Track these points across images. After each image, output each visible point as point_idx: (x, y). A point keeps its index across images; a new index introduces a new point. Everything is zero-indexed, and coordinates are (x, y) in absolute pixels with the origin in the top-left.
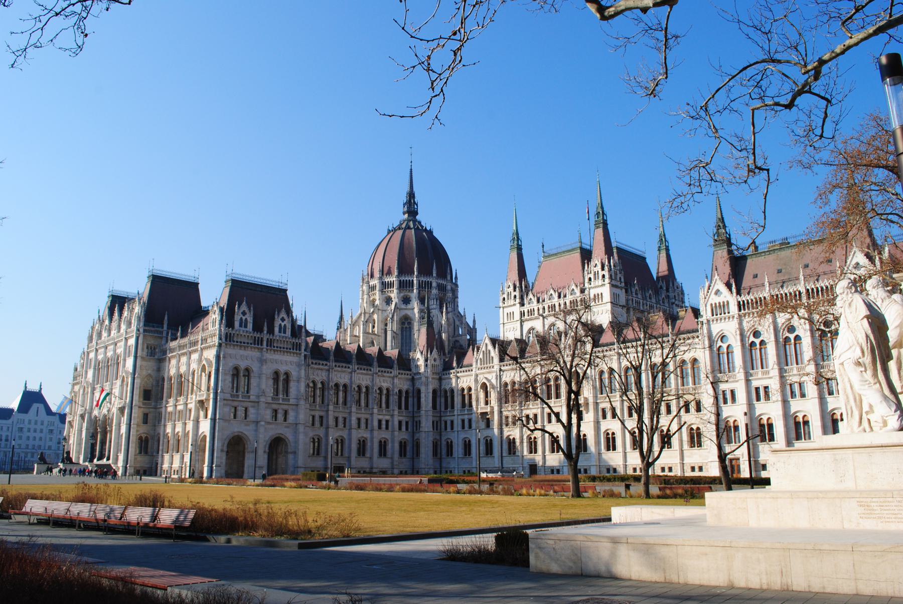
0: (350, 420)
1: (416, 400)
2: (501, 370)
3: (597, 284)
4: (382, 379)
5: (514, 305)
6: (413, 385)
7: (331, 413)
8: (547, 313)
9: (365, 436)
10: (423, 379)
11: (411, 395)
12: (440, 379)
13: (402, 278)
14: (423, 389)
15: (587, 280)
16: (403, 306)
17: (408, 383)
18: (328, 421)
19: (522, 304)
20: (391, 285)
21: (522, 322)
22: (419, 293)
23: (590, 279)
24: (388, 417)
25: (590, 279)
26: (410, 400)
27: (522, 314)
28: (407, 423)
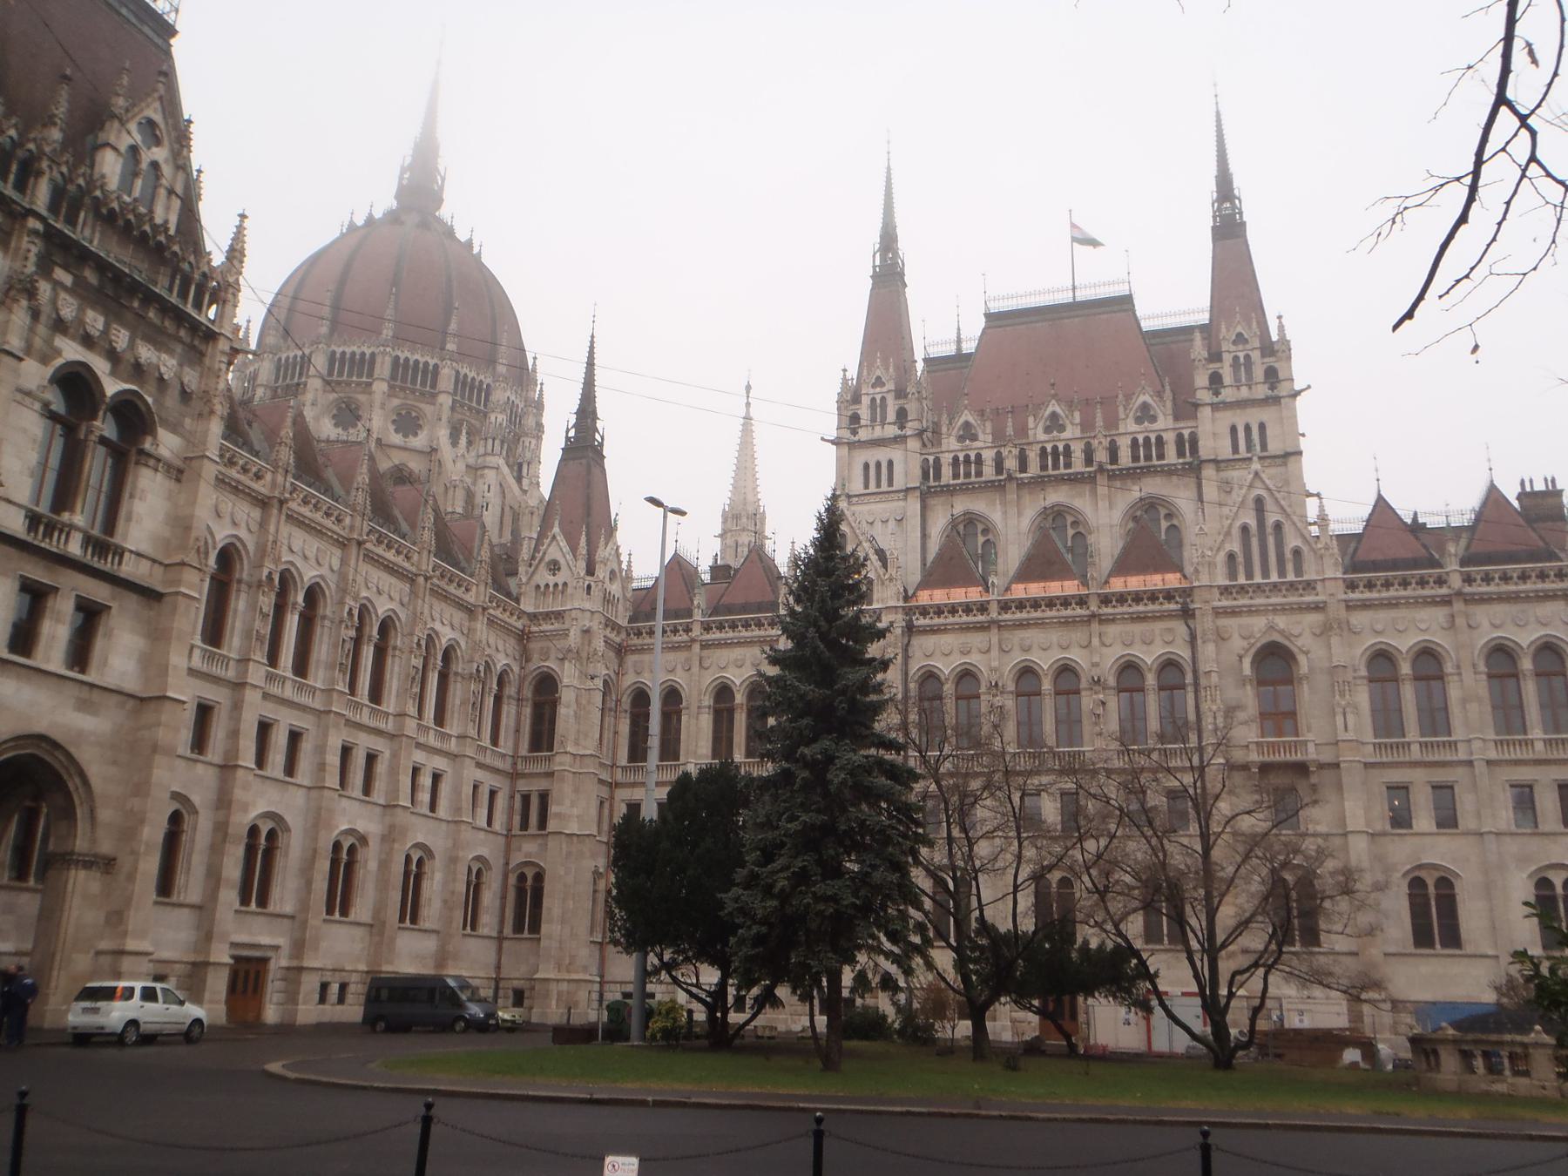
0: (321, 749)
1: (527, 711)
2: (910, 629)
3: (1244, 393)
4: (439, 606)
5: (899, 440)
6: (525, 656)
7: (252, 697)
8: (1034, 469)
9: (361, 826)
10: (574, 638)
11: (510, 690)
12: (621, 651)
13: (403, 354)
14: (568, 676)
15: (1201, 380)
16: (397, 439)
17: (511, 644)
18: (234, 734)
19: (930, 436)
20: (364, 365)
21: (926, 495)
22: (453, 409)
23: (1216, 379)
24: (440, 763)
25: (1216, 379)
26: (509, 711)
27: (930, 470)
28: (493, 794)
